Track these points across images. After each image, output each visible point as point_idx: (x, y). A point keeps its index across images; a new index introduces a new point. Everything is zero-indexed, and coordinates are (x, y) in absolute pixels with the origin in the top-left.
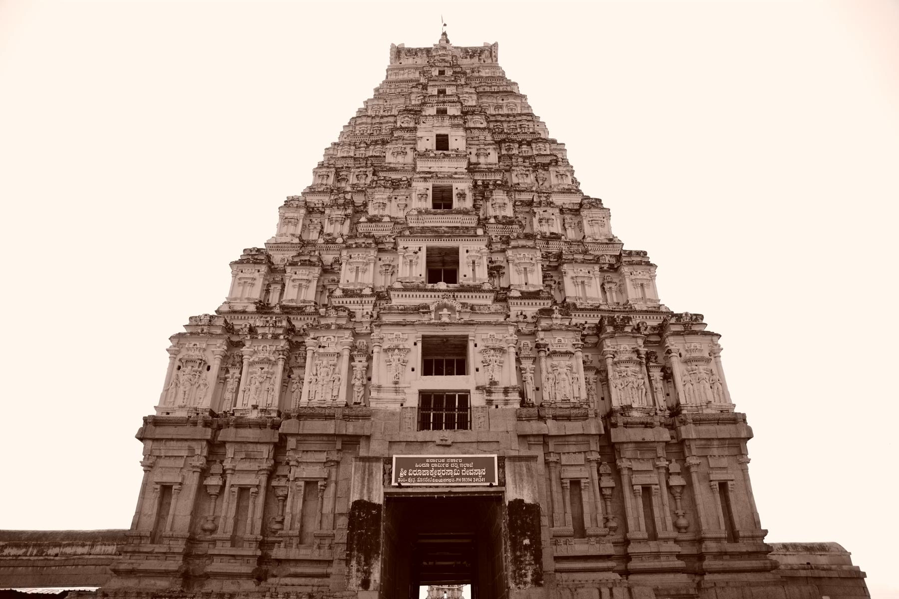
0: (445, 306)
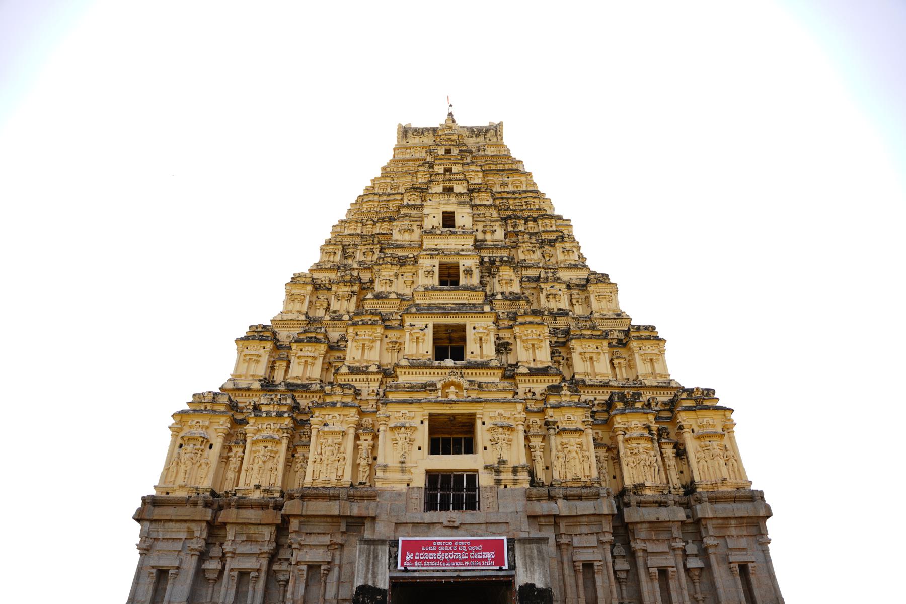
0: (453, 383)
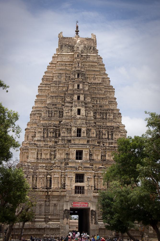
0: (80, 167)
